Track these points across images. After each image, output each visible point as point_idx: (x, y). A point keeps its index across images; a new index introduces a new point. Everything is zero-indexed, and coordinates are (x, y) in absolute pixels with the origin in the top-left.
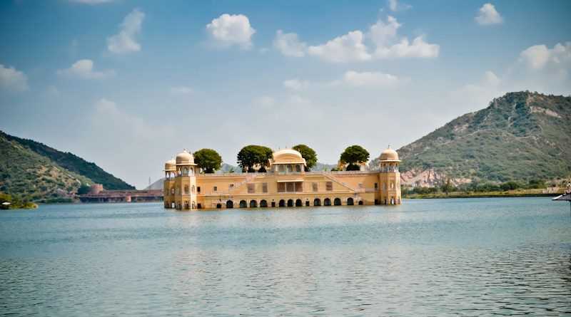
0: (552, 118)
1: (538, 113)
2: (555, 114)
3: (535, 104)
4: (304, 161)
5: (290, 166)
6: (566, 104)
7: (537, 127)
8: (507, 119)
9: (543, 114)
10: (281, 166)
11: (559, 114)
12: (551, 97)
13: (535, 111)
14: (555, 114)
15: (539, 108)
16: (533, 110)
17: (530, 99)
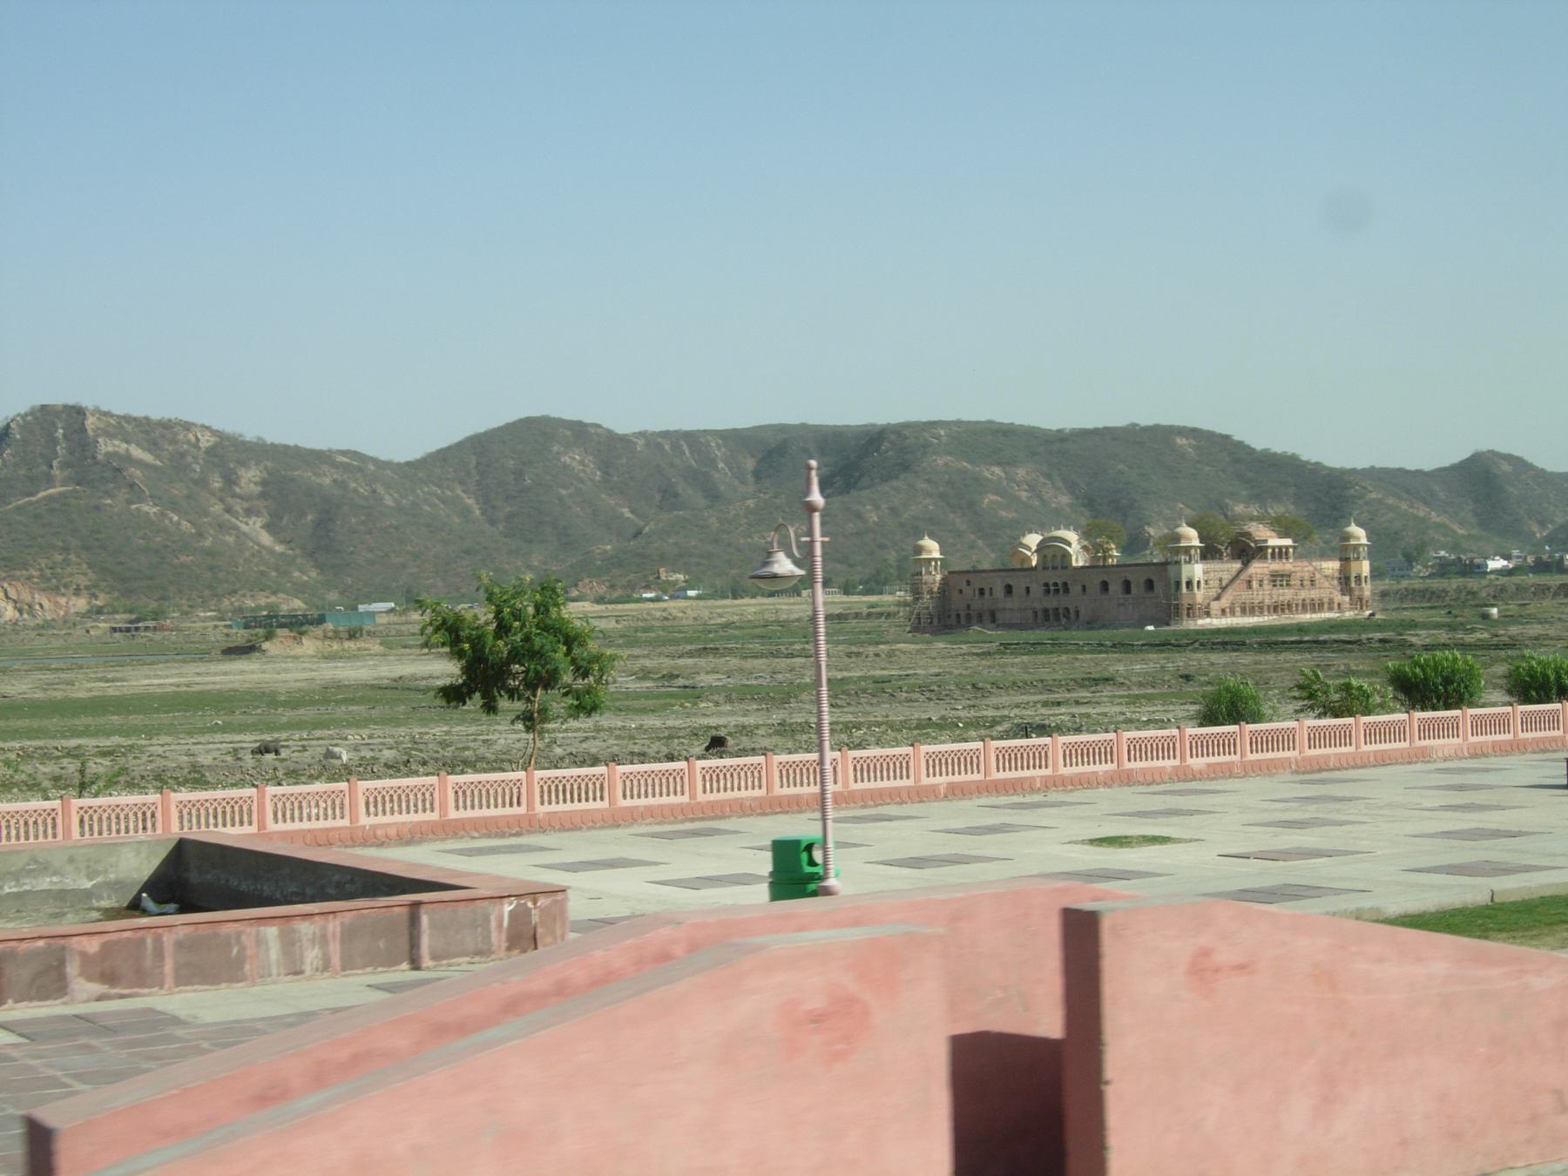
0: (141, 464)
1: (116, 454)
2: (147, 457)
3: (111, 436)
4: (1288, 542)
5: (1280, 548)
6: (163, 436)
7: (132, 486)
8: (51, 467)
9: (128, 458)
10: (1274, 548)
11: (157, 457)
12: (128, 419)
13: (110, 449)
14: (147, 457)
15: (116, 442)
16: (105, 446)
17: (91, 422)
